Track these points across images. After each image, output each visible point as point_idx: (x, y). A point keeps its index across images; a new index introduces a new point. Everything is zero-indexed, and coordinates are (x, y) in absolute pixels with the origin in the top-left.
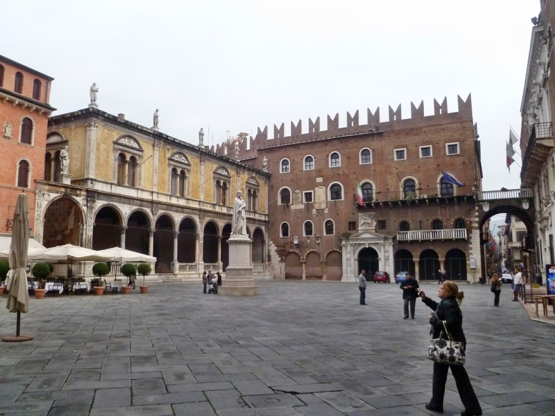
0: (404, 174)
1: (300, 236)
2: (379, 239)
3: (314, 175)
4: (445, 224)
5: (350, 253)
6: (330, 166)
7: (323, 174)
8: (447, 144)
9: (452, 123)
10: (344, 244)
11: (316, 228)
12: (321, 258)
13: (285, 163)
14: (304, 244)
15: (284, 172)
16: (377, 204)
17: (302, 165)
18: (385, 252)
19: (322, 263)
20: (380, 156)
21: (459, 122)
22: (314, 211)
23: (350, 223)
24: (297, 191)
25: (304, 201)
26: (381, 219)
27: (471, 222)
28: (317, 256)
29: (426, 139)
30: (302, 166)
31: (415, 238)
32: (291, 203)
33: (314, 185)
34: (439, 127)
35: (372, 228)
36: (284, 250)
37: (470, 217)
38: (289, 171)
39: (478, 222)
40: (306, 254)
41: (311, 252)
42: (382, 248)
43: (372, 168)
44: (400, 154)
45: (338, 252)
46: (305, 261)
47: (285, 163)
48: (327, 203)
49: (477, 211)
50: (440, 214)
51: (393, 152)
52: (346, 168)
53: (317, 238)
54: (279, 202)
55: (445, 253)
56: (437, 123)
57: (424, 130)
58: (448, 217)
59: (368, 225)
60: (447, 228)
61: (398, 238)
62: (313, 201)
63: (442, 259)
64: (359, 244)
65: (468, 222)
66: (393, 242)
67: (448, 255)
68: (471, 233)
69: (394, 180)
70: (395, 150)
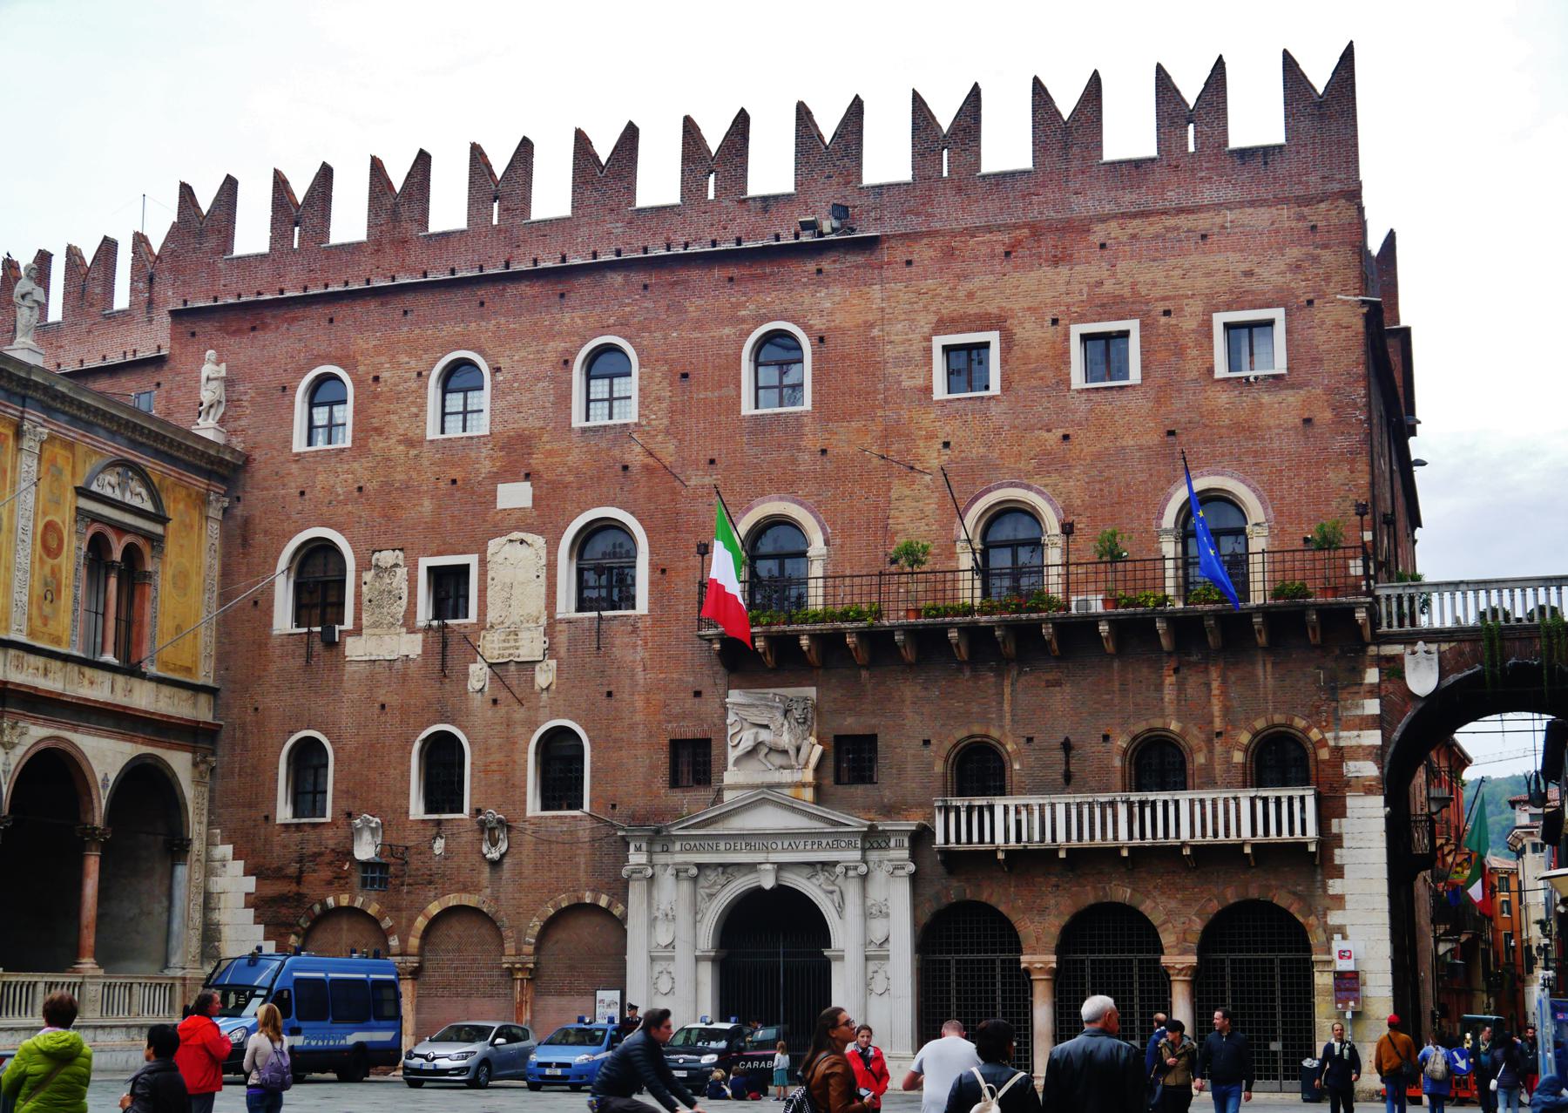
0: (979, 475)
1: (394, 817)
2: (837, 837)
3: (486, 467)
4: (1200, 759)
5: (670, 918)
6: (578, 421)
7: (536, 461)
8: (1219, 319)
9: (1252, 204)
10: (638, 870)
11: (483, 770)
12: (510, 947)
13: (323, 391)
14: (415, 862)
15: (320, 444)
16: (830, 643)
17: (422, 407)
18: (867, 915)
19: (511, 972)
20: (854, 373)
21: (1285, 201)
22: (478, 675)
23: (676, 746)
24: (386, 557)
25: (424, 613)
26: (851, 724)
27: (1340, 754)
28: (485, 931)
29: (1109, 286)
30: (419, 416)
31: (1033, 838)
32: (348, 624)
33: (485, 524)
34: (1184, 221)
35: (797, 776)
36: (300, 897)
37: (1338, 722)
38: (345, 439)
39: (1377, 754)
40: (421, 923)
41: (448, 912)
42: (852, 890)
43: (812, 440)
44: (966, 363)
45: (606, 912)
46: (413, 962)
47: (323, 391)
48: (550, 631)
49: (1374, 691)
50: (1170, 703)
51: (929, 350)
52: (667, 433)
53: (487, 830)
54: (283, 619)
55: (1198, 926)
56: (1172, 197)
57: (1099, 233)
58: (1218, 724)
59: (777, 760)
60: (1210, 783)
61: (940, 838)
62: (473, 617)
63: (1178, 958)
64: (725, 866)
65: (1324, 754)
66: (914, 857)
67: (1212, 939)
68: (1342, 814)
69: (931, 507)
70: (939, 342)
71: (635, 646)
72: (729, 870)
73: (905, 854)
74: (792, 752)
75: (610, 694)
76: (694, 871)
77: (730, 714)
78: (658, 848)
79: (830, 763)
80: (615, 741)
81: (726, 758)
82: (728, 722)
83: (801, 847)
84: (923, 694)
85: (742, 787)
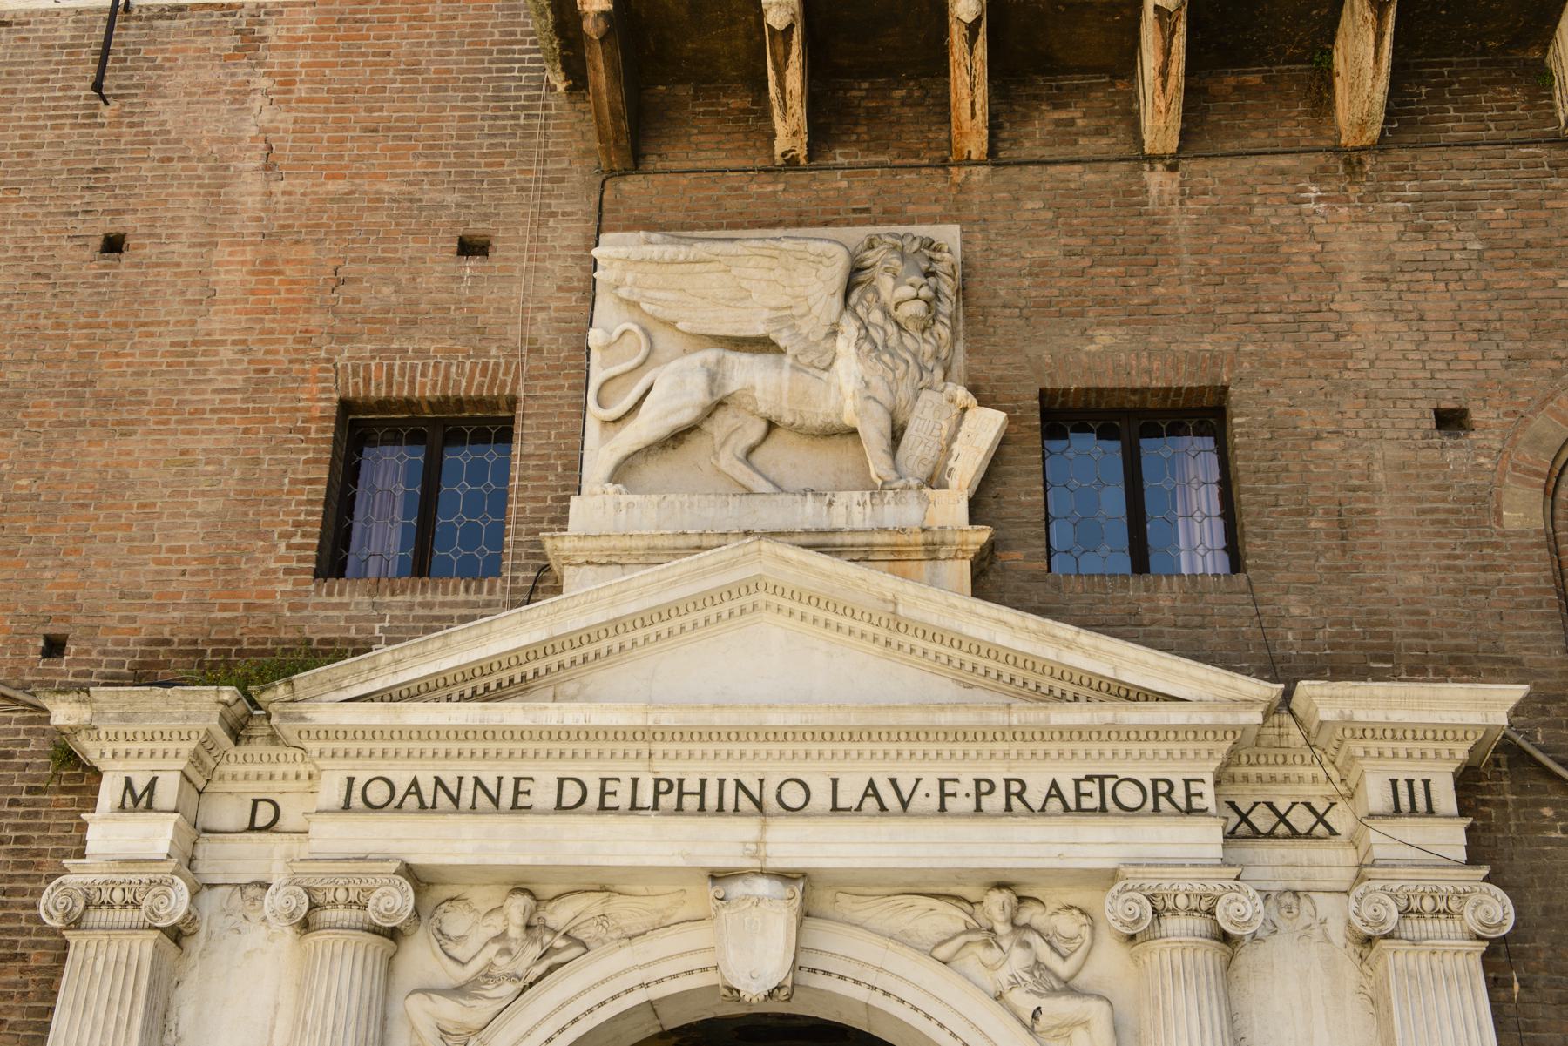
23: (359, 428)
35: (904, 513)
71: (241, 94)
72: (560, 915)
73: (1451, 837)
74: (874, 434)
75: (113, 244)
76: (396, 901)
80: (104, 401)
81: (575, 467)
82: (595, 337)
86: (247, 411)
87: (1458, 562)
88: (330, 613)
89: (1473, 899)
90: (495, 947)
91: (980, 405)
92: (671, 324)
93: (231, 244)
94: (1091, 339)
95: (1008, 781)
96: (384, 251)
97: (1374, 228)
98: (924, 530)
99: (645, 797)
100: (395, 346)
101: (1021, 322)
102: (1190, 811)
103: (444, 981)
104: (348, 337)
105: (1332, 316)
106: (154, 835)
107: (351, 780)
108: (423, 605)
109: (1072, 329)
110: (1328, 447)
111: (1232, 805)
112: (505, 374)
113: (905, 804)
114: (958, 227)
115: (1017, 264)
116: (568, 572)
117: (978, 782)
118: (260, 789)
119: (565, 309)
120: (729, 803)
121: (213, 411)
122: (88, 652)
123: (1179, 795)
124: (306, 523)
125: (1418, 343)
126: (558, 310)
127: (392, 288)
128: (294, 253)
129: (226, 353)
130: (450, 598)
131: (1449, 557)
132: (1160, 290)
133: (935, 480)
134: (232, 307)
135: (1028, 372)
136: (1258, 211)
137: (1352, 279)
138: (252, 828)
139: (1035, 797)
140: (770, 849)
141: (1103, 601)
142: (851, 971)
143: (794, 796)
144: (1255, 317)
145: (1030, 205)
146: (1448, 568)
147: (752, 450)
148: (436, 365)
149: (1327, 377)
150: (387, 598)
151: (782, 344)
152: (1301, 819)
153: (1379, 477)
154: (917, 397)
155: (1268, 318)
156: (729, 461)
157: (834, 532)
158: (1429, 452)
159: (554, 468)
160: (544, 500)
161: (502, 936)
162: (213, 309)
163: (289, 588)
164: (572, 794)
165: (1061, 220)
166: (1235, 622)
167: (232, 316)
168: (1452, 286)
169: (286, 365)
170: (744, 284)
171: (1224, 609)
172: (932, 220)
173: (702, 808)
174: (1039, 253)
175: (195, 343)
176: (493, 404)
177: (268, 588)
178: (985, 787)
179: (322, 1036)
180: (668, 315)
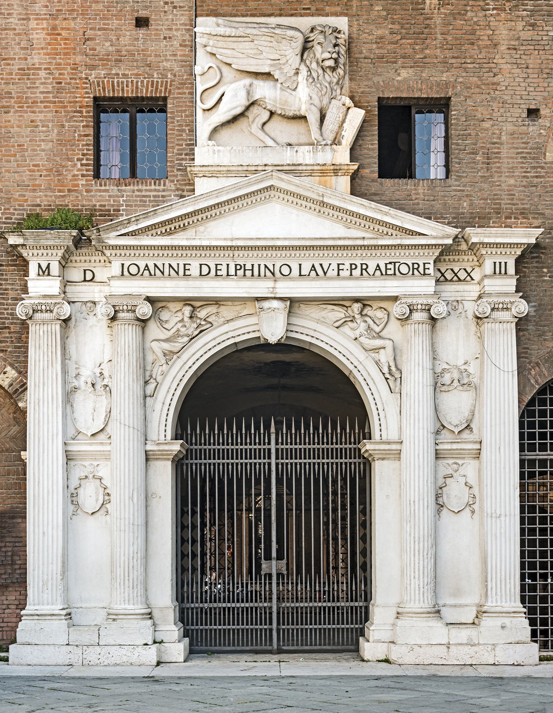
5: (100, 385)
23: (102, 106)
26: (404, 81)
35: (325, 157)
42: (413, 342)
72: (202, 314)
74: (313, 118)
77: (200, 53)
78: (76, 274)
79: (372, 145)
81: (193, 131)
82: (198, 70)
83: (332, 273)
84: (527, 35)
85: (228, 173)
86: (55, 102)
87: (528, 174)
88: (102, 194)
89: (516, 304)
90: (180, 325)
91: (355, 106)
92: (230, 65)
93: (36, 19)
94: (399, 75)
95: (362, 264)
96: (104, 24)
97: (513, 23)
98: (333, 165)
99: (232, 271)
100: (113, 72)
101: (371, 66)
102: (425, 274)
103: (163, 337)
104: (93, 67)
105: (494, 65)
106: (51, 286)
107: (123, 265)
108: (139, 190)
109: (391, 69)
110: (486, 125)
111: (439, 270)
112: (161, 86)
113: (325, 273)
114: (347, 18)
115: (371, 37)
116: (196, 180)
117: (351, 264)
118: (86, 266)
119: (184, 55)
120: (262, 274)
121: (41, 102)
122: (8, 209)
123: (421, 269)
124: (87, 154)
125: (525, 78)
126: (181, 56)
127: (109, 43)
128: (64, 24)
129: (43, 74)
130: (148, 188)
131: (525, 172)
132: (427, 51)
133: (336, 141)
134: (41, 51)
135: (374, 90)
136: (469, 14)
137: (503, 48)
138: (85, 280)
139: (371, 270)
140: (277, 290)
141: (398, 190)
142: (305, 331)
143: (285, 270)
144: (464, 65)
145: (377, 8)
146: (524, 177)
147: (264, 124)
148: (132, 82)
149: (489, 94)
150: (124, 188)
151: (276, 77)
152: (462, 275)
153: (504, 138)
154: (330, 103)
155: (469, 66)
156: (255, 128)
157: (299, 165)
158: (523, 127)
159: (183, 131)
160: (182, 145)
161: (182, 321)
162: (33, 52)
163: (84, 183)
164: (205, 270)
165: (390, 16)
166: (446, 199)
167: (42, 56)
168: (541, 52)
169: (69, 81)
170: (260, 48)
171: (442, 194)
172: (336, 14)
173: (253, 275)
174: (380, 32)
175: (28, 69)
176: (157, 99)
177: (76, 182)
178: (354, 267)
179: (125, 357)
180: (228, 61)
